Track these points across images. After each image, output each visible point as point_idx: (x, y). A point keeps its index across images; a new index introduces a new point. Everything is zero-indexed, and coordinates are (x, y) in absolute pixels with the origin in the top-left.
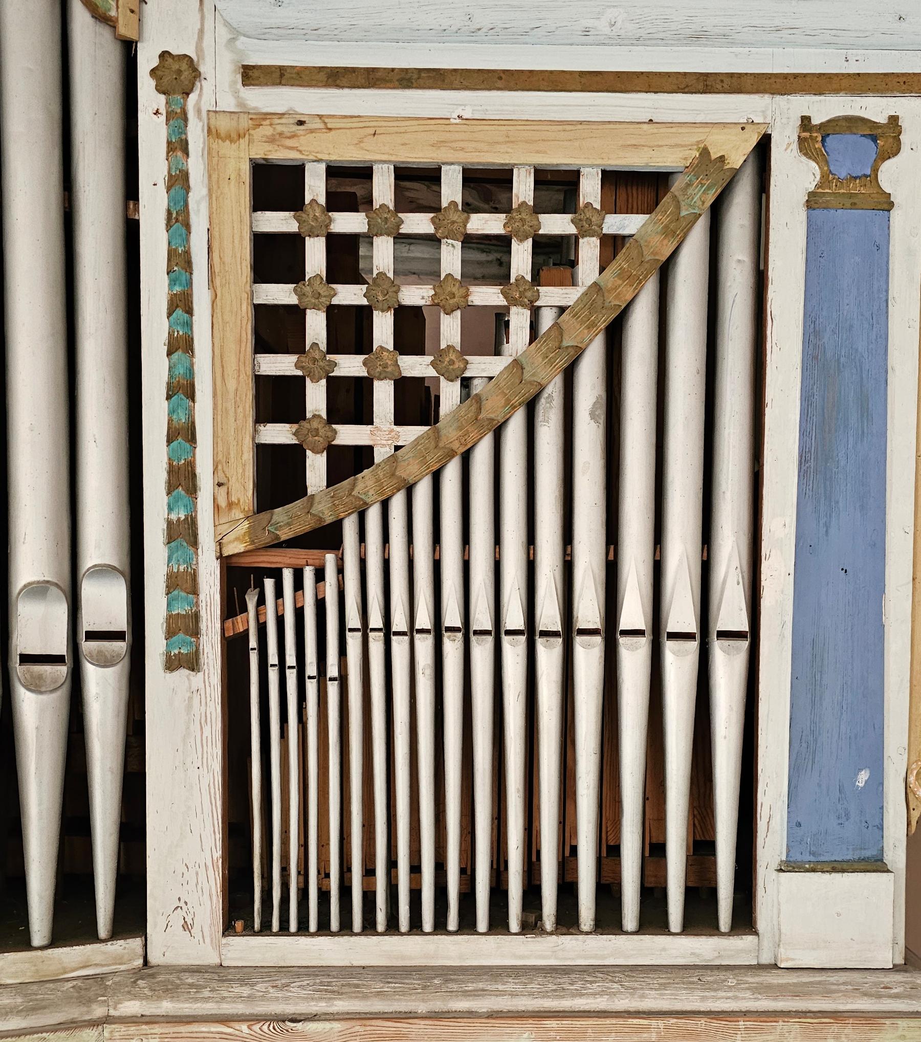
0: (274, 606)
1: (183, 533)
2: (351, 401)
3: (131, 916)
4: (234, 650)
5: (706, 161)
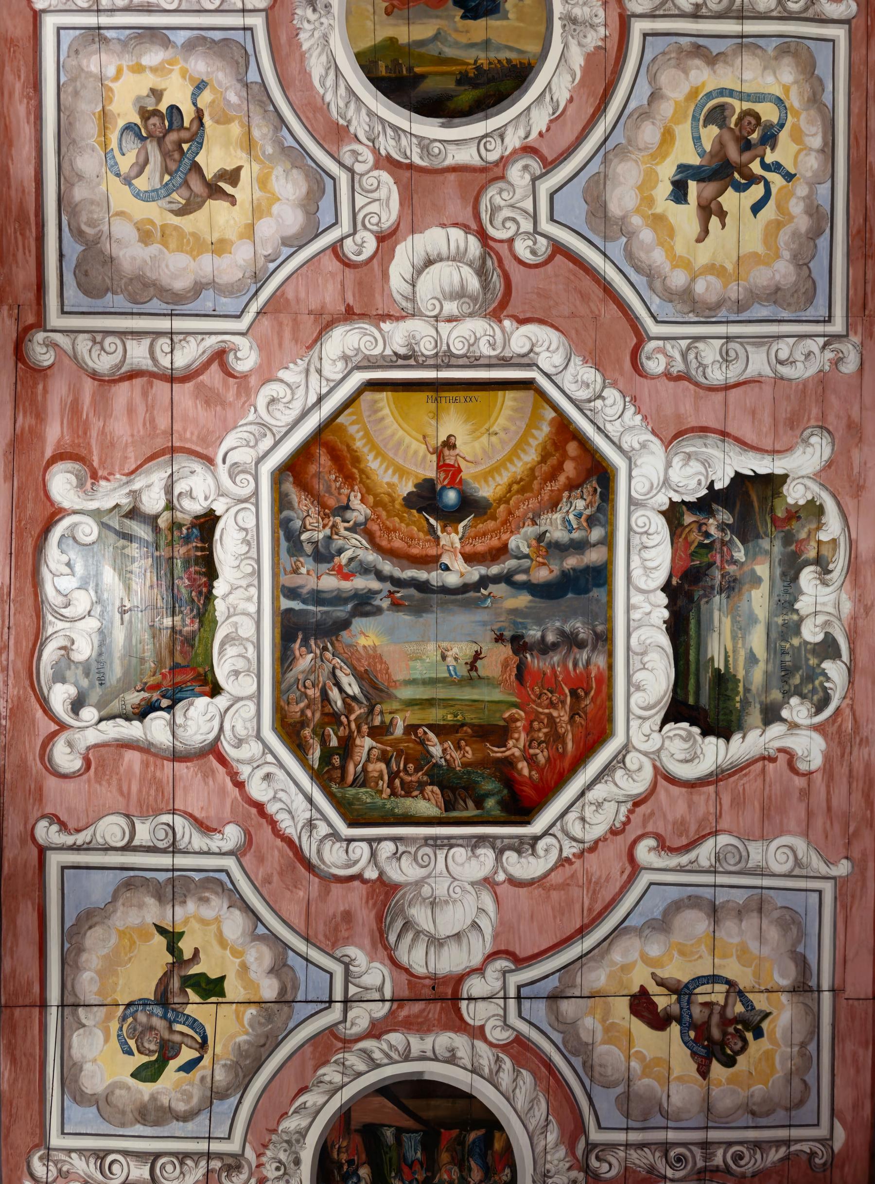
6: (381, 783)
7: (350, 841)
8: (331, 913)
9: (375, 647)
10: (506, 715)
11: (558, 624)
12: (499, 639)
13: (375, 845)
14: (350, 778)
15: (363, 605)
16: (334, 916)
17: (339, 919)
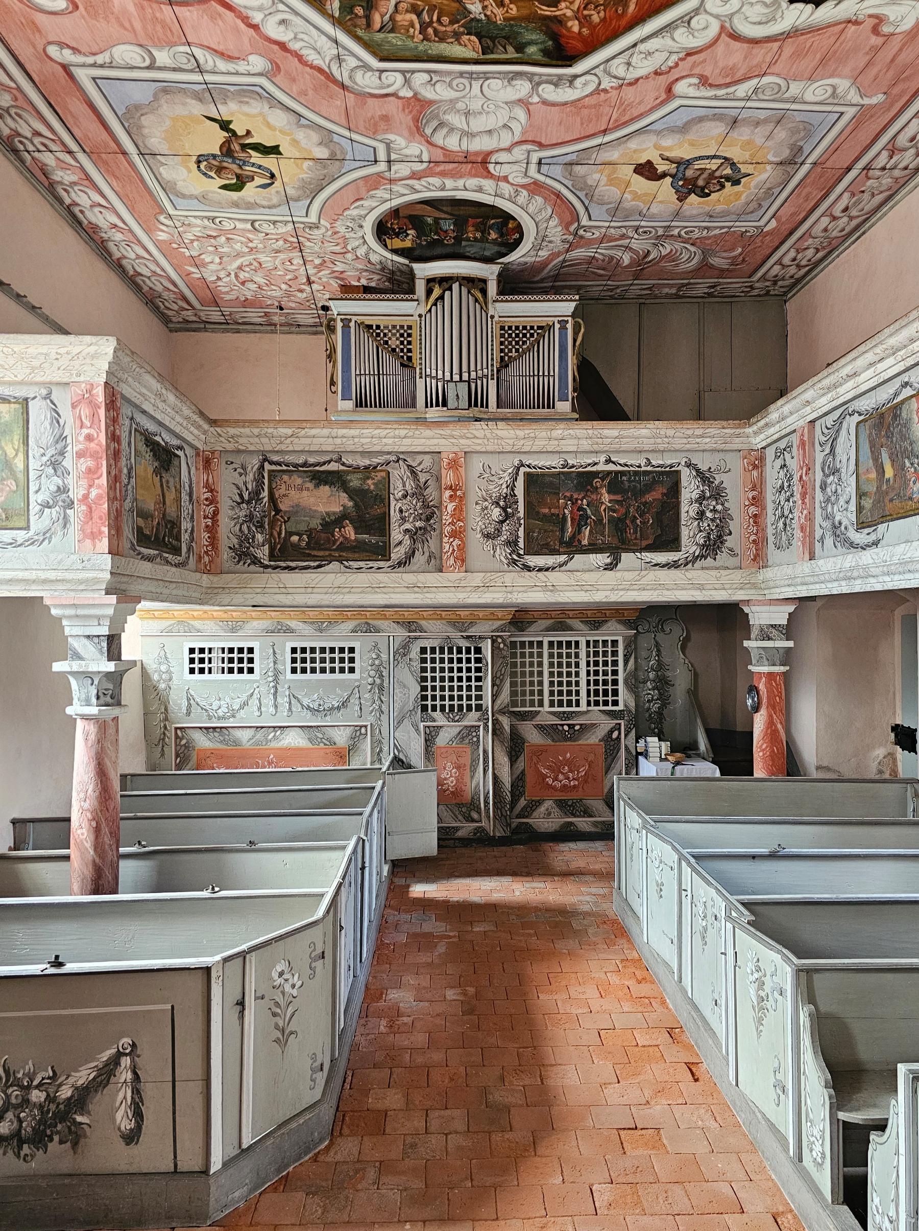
1: (492, 365)
3: (487, 407)
4: (498, 378)
5: (548, 325)
6: (412, 30)
7: (382, 71)
8: (369, 115)
13: (408, 76)
14: (377, 26)
16: (373, 117)
17: (377, 119)
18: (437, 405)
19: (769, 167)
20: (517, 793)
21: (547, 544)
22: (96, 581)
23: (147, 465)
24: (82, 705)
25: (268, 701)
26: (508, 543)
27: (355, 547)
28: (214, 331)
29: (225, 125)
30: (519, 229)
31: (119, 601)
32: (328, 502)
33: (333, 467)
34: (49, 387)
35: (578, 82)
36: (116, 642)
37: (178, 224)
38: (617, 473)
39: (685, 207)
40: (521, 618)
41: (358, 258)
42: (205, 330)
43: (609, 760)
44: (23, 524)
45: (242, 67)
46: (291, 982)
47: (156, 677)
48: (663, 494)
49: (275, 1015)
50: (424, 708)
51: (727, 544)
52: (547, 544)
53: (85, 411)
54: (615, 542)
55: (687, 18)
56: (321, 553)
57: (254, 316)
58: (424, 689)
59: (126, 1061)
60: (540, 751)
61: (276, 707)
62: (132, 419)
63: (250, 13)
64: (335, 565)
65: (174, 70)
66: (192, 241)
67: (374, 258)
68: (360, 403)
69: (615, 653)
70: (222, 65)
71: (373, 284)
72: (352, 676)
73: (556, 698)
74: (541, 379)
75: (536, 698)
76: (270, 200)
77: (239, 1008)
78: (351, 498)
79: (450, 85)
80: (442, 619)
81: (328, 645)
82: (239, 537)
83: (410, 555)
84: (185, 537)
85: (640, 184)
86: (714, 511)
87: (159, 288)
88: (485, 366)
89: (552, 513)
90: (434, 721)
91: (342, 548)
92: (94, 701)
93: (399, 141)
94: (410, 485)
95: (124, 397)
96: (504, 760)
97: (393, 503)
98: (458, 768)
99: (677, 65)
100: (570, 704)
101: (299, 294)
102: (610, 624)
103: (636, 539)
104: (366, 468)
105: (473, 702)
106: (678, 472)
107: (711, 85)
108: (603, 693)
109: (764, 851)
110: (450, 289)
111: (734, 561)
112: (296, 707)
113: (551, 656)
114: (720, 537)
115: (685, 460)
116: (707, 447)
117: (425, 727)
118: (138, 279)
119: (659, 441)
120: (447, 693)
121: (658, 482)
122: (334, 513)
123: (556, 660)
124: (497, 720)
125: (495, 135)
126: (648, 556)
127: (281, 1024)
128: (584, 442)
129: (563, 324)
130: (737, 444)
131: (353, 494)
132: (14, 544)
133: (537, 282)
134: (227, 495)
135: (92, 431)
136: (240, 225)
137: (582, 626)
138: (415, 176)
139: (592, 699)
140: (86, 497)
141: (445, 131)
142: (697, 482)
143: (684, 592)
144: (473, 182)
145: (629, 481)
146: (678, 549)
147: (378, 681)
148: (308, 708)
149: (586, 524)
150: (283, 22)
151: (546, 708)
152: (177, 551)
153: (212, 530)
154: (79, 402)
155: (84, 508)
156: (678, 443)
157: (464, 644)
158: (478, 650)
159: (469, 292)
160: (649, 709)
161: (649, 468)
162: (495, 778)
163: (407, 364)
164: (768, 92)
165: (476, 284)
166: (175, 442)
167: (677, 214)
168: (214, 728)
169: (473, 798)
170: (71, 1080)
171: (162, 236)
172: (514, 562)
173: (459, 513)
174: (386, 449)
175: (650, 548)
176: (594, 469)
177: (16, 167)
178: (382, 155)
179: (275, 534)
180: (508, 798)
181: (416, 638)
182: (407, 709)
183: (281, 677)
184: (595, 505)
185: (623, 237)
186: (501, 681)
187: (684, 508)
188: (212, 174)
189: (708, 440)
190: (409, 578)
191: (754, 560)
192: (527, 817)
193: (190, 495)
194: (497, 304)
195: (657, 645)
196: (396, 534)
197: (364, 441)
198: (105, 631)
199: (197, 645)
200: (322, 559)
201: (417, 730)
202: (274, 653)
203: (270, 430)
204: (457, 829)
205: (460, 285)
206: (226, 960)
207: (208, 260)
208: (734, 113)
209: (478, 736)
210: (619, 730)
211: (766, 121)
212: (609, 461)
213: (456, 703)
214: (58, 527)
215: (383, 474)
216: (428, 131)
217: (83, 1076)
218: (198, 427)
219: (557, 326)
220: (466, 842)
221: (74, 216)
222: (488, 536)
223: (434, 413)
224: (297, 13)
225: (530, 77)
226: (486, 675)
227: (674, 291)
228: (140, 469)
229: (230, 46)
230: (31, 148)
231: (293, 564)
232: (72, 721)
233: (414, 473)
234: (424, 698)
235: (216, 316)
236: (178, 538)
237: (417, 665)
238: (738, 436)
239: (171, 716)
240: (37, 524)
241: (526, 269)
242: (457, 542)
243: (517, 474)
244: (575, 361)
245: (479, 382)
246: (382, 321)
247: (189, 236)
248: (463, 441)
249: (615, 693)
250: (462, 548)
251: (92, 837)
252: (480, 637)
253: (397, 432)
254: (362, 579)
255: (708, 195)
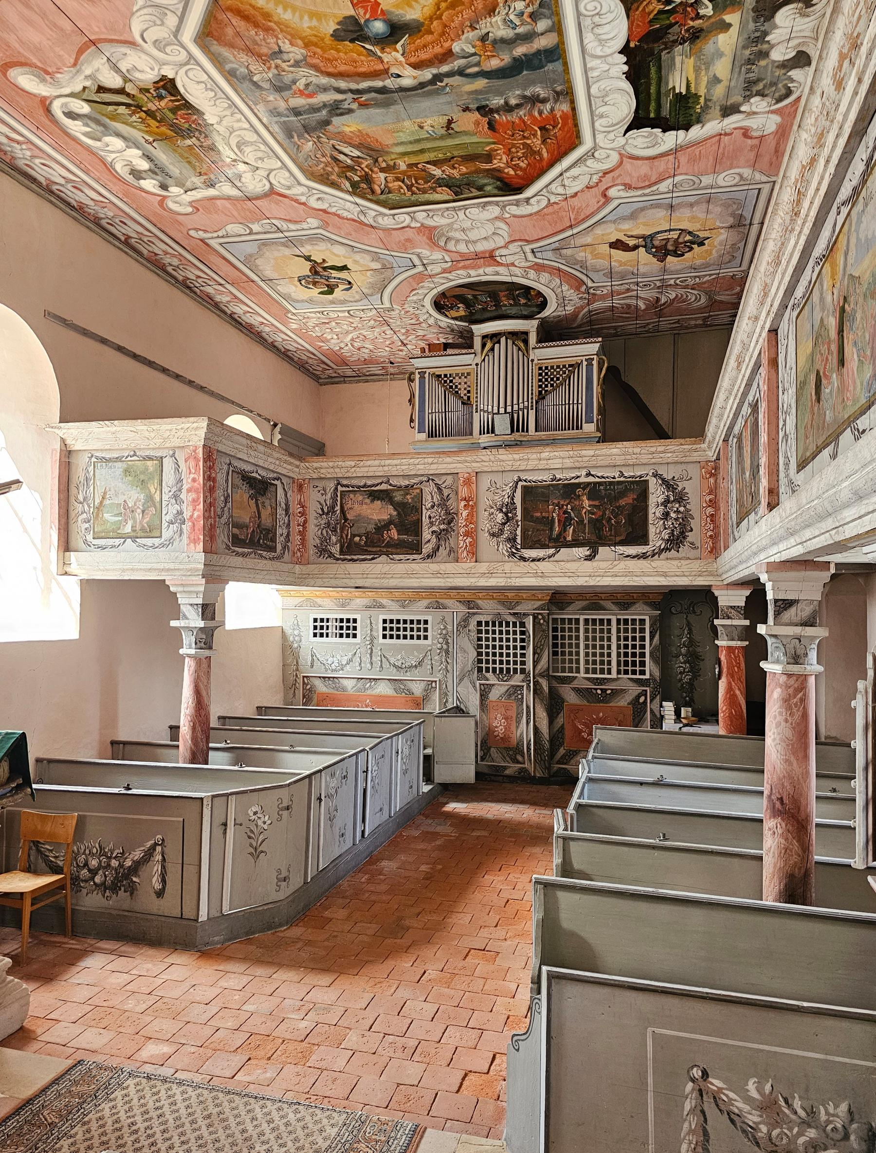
0: (540, 403)
1: (532, 398)
2: (546, 386)
3: (527, 431)
7: (394, 215)
9: (359, 131)
10: (487, 149)
11: (517, 92)
12: (466, 109)
14: (379, 192)
15: (336, 109)
16: (400, 241)
18: (488, 433)
19: (722, 231)
20: (558, 743)
21: (539, 540)
22: (197, 570)
23: (243, 493)
24: (188, 648)
25: (366, 659)
26: (509, 540)
27: (397, 544)
28: (350, 382)
29: (308, 258)
30: (540, 294)
31: (207, 583)
32: (380, 512)
33: (384, 487)
34: (174, 449)
35: (532, 201)
36: (210, 608)
37: (301, 318)
38: (595, 483)
39: (668, 266)
40: (559, 598)
41: (430, 326)
42: (345, 382)
43: (636, 721)
44: (158, 534)
45: (305, 226)
46: (263, 819)
47: (291, 639)
48: (634, 499)
49: (250, 837)
50: (480, 670)
51: (688, 539)
52: (539, 540)
53: (192, 463)
54: (594, 538)
55: (590, 154)
56: (374, 549)
57: (375, 369)
58: (480, 654)
59: (159, 849)
60: (576, 710)
61: (372, 663)
62: (230, 464)
63: (298, 198)
64: (384, 558)
65: (265, 233)
66: (314, 327)
67: (442, 324)
68: (431, 435)
69: (642, 630)
70: (292, 227)
71: (450, 341)
72: (426, 642)
73: (590, 666)
74: (575, 407)
75: (574, 665)
76: (354, 297)
77: (223, 827)
78: (395, 509)
79: (442, 216)
80: (493, 599)
81: (408, 618)
82: (320, 539)
83: (436, 549)
84: (280, 540)
85: (617, 254)
86: (678, 512)
87: (305, 358)
88: (526, 399)
89: (544, 517)
90: (487, 680)
91: (388, 545)
92: (194, 645)
93: (425, 252)
94: (437, 498)
95: (218, 451)
96: (542, 715)
97: (424, 511)
98: (506, 718)
99: (601, 181)
100: (602, 671)
101: (400, 353)
102: (637, 605)
103: (611, 535)
104: (406, 487)
105: (518, 667)
106: (647, 481)
107: (636, 188)
108: (630, 663)
109: (651, 780)
110: (499, 342)
111: (697, 553)
112: (386, 664)
113: (586, 631)
114: (682, 533)
115: (652, 471)
116: (669, 460)
117: (480, 684)
118: (289, 353)
119: (628, 457)
120: (497, 658)
121: (631, 490)
122: (384, 520)
123: (590, 635)
124: (538, 681)
125: (491, 240)
126: (621, 549)
127: (254, 844)
128: (567, 461)
129: (590, 361)
130: (695, 457)
131: (397, 506)
132: (153, 547)
133: (574, 328)
134: (313, 508)
135: (196, 476)
136: (341, 315)
137: (613, 607)
138: (444, 271)
139: (622, 668)
140: (191, 516)
141: (453, 242)
142: (663, 488)
143: (651, 578)
144: (489, 270)
145: (605, 489)
146: (646, 543)
147: (445, 647)
148: (394, 666)
149: (570, 524)
150: (319, 199)
151: (582, 674)
152: (273, 549)
153: (302, 534)
154: (189, 458)
155: (190, 524)
156: (645, 459)
157: (511, 619)
158: (523, 625)
159: (513, 343)
160: (681, 680)
161: (622, 479)
162: (536, 728)
163: (467, 403)
164: (686, 186)
165: (521, 337)
166: (272, 475)
167: (665, 270)
168: (329, 678)
169: (518, 744)
170: (131, 856)
171: (294, 326)
172: (513, 554)
173: (472, 518)
174: (419, 473)
175: (622, 543)
176: (577, 481)
177: (192, 298)
178: (417, 262)
179: (344, 536)
180: (547, 745)
181: (474, 614)
182: (466, 670)
183: (375, 641)
184: (577, 509)
185: (628, 290)
186: (541, 650)
187: (651, 510)
188: (311, 286)
189: (670, 455)
190: (433, 567)
191: (711, 552)
192: (565, 764)
193: (287, 510)
194: (536, 351)
195: (689, 624)
196: (426, 535)
197: (403, 467)
198: (200, 601)
199: (319, 617)
200: (375, 553)
201: (474, 686)
202: (371, 623)
203: (340, 463)
204: (505, 768)
205: (507, 339)
206: (213, 797)
207: (329, 337)
208: (669, 201)
209: (522, 694)
210: (646, 696)
211: (697, 203)
212: (589, 474)
213: (504, 666)
214: (177, 536)
215: (418, 491)
216: (442, 244)
217: (137, 854)
218: (290, 464)
219: (585, 363)
220: (512, 779)
221: (236, 320)
222: (493, 535)
223: (485, 440)
224: (326, 193)
225: (497, 204)
226: (529, 644)
227: (700, 322)
228: (237, 497)
229: (293, 216)
230: (198, 285)
231: (355, 557)
232: (183, 658)
233: (439, 489)
234: (480, 661)
235: (349, 373)
236: (273, 540)
237: (474, 635)
238: (696, 450)
239: (301, 667)
240: (167, 534)
241: (562, 320)
242: (469, 540)
243: (516, 487)
244: (600, 390)
245: (521, 413)
246: (448, 371)
247: (310, 324)
248: (474, 465)
249: (643, 664)
250: (474, 545)
251: (190, 732)
252: (524, 614)
253: (426, 460)
254: (400, 568)
255: (682, 255)
